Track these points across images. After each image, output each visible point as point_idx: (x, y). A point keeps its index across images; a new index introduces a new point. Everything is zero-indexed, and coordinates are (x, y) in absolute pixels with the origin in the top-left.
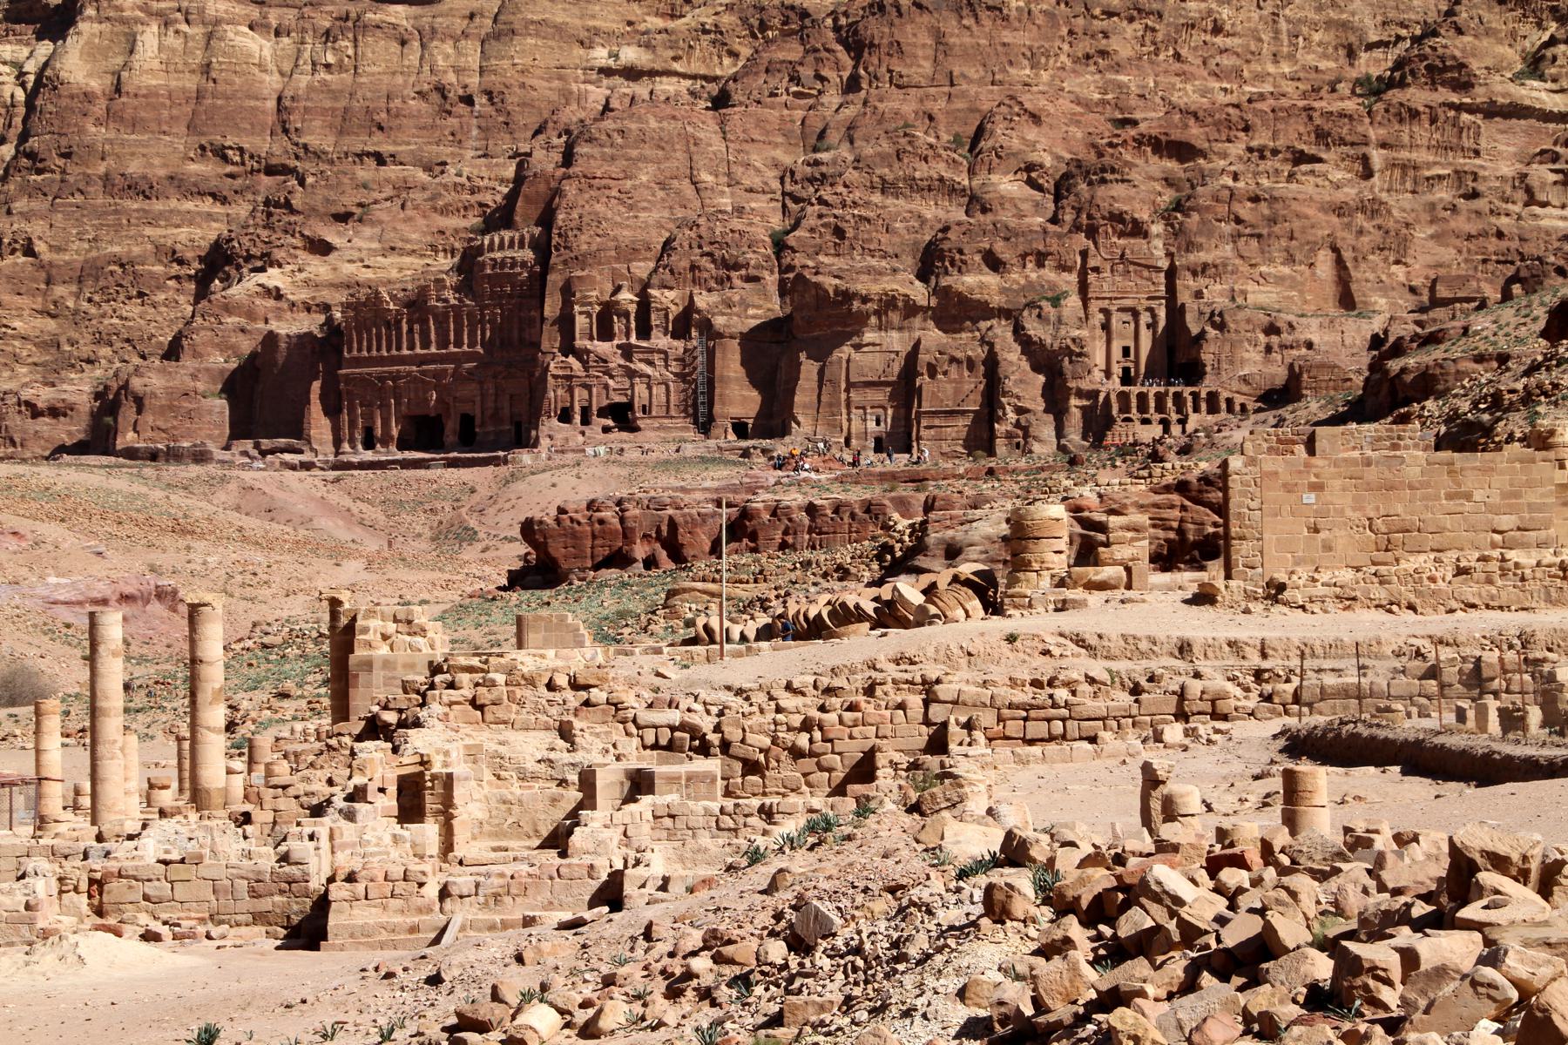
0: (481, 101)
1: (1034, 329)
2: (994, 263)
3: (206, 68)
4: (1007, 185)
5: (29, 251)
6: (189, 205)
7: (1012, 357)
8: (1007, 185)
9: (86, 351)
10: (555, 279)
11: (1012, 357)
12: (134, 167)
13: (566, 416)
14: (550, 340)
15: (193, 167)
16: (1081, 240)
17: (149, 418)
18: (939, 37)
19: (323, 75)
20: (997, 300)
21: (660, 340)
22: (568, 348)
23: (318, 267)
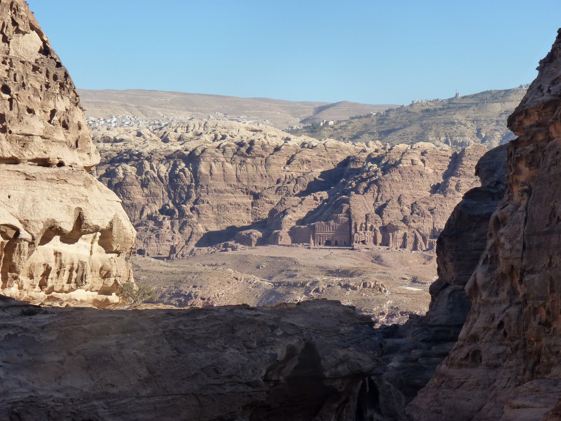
0: (268, 176)
1: (421, 231)
2: (414, 222)
3: (224, 170)
4: (406, 208)
5: (208, 203)
6: (229, 195)
7: (418, 235)
8: (406, 208)
9: (222, 220)
10: (353, 222)
11: (418, 235)
12: (219, 188)
13: (356, 242)
14: (353, 231)
15: (227, 188)
16: (423, 218)
17: (282, 240)
18: (390, 185)
19: (242, 172)
20: (415, 227)
21: (368, 231)
22: (356, 232)
23: (295, 215)
